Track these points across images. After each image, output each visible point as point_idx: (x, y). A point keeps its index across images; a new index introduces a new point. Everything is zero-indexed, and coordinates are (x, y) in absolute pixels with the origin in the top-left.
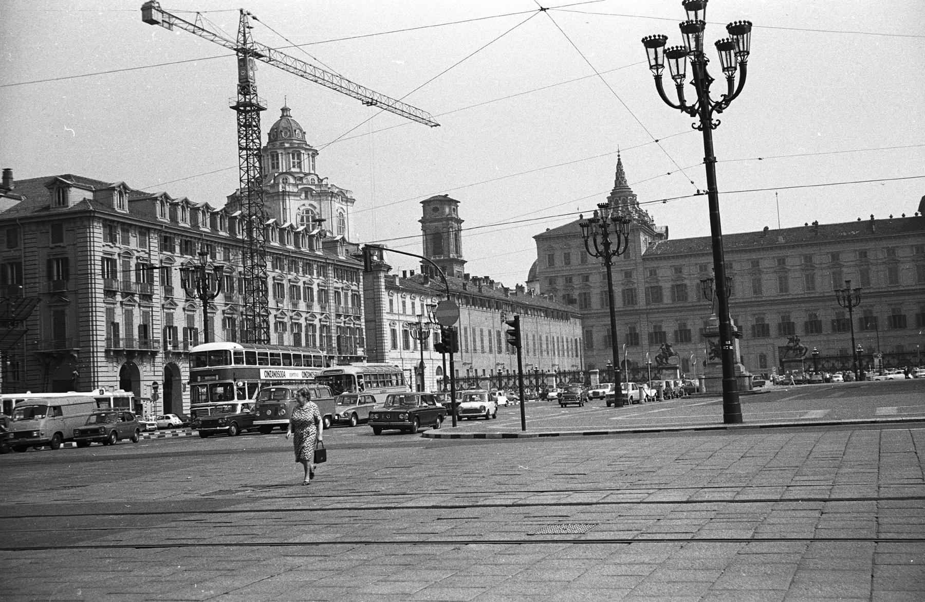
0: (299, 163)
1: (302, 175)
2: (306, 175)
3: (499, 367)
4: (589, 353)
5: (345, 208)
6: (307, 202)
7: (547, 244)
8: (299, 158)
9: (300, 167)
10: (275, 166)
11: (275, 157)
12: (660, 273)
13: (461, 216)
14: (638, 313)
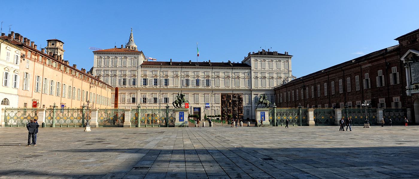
14: (137, 89)
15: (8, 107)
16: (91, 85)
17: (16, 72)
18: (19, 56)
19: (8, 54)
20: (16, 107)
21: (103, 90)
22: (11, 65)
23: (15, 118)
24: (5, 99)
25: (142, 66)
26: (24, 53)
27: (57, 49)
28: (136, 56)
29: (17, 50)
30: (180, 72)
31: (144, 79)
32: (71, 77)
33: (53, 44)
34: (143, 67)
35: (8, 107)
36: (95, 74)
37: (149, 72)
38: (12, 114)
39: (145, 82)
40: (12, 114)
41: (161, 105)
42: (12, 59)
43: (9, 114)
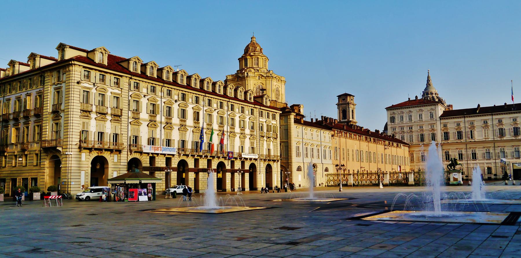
0: (258, 63)
1: (258, 69)
3: (363, 169)
4: (412, 164)
6: (260, 81)
7: (392, 111)
8: (258, 61)
9: (258, 65)
10: (246, 65)
11: (246, 60)
12: (449, 126)
13: (355, 103)
16: (386, 147)
20: (333, 173)
21: (398, 149)
25: (443, 117)
26: (333, 133)
27: (349, 104)
28: (433, 107)
30: (492, 119)
31: (445, 133)
32: (367, 143)
33: (344, 100)
34: (443, 119)
36: (390, 133)
37: (452, 123)
39: (446, 136)
40: (332, 178)
41: (469, 162)
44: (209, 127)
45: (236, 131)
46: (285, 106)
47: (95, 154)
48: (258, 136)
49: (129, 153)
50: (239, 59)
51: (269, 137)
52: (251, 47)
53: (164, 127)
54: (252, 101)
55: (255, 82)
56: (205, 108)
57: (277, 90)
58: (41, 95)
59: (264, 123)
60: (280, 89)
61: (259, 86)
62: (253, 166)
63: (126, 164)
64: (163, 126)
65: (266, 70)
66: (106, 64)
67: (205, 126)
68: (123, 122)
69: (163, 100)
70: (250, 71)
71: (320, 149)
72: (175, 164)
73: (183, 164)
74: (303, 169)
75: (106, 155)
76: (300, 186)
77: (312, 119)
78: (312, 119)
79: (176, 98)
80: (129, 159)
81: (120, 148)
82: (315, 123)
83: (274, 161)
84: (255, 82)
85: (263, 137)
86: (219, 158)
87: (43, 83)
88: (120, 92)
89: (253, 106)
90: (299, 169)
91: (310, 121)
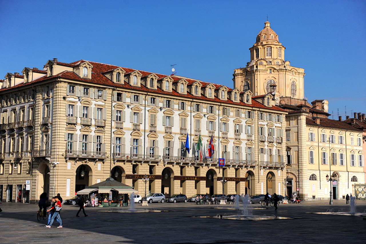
1: (271, 60)
2: (274, 59)
5: (297, 79)
6: (271, 75)
15: (356, 183)
17: (360, 152)
18: (361, 138)
19: (352, 139)
22: (355, 148)
23: (363, 192)
24: (354, 177)
29: (359, 133)
35: (356, 183)
38: (360, 189)
40: (360, 189)
42: (356, 142)
43: (358, 189)
44: (197, 133)
45: (229, 137)
46: (303, 103)
47: (79, 163)
48: (257, 141)
49: (112, 162)
50: (250, 49)
51: (270, 142)
52: (264, 35)
53: (148, 136)
54: (250, 102)
55: (266, 76)
56: (193, 114)
57: (293, 85)
58: (33, 107)
59: (266, 126)
60: (297, 83)
61: (271, 81)
62: (250, 173)
63: (109, 172)
64: (147, 134)
65: (280, 61)
66: (90, 78)
67: (193, 133)
68: (106, 132)
69: (147, 109)
70: (261, 64)
71: (344, 154)
72: (159, 171)
73: (167, 171)
74: (318, 178)
75: (91, 164)
76: (314, 197)
77: (340, 117)
78: (340, 117)
79: (161, 105)
80: (113, 167)
81: (103, 157)
82: (344, 122)
83: (277, 168)
84: (266, 76)
85: (264, 142)
86: (207, 165)
87: (34, 98)
88: (103, 104)
89: (251, 108)
90: (313, 177)
91: (338, 119)
